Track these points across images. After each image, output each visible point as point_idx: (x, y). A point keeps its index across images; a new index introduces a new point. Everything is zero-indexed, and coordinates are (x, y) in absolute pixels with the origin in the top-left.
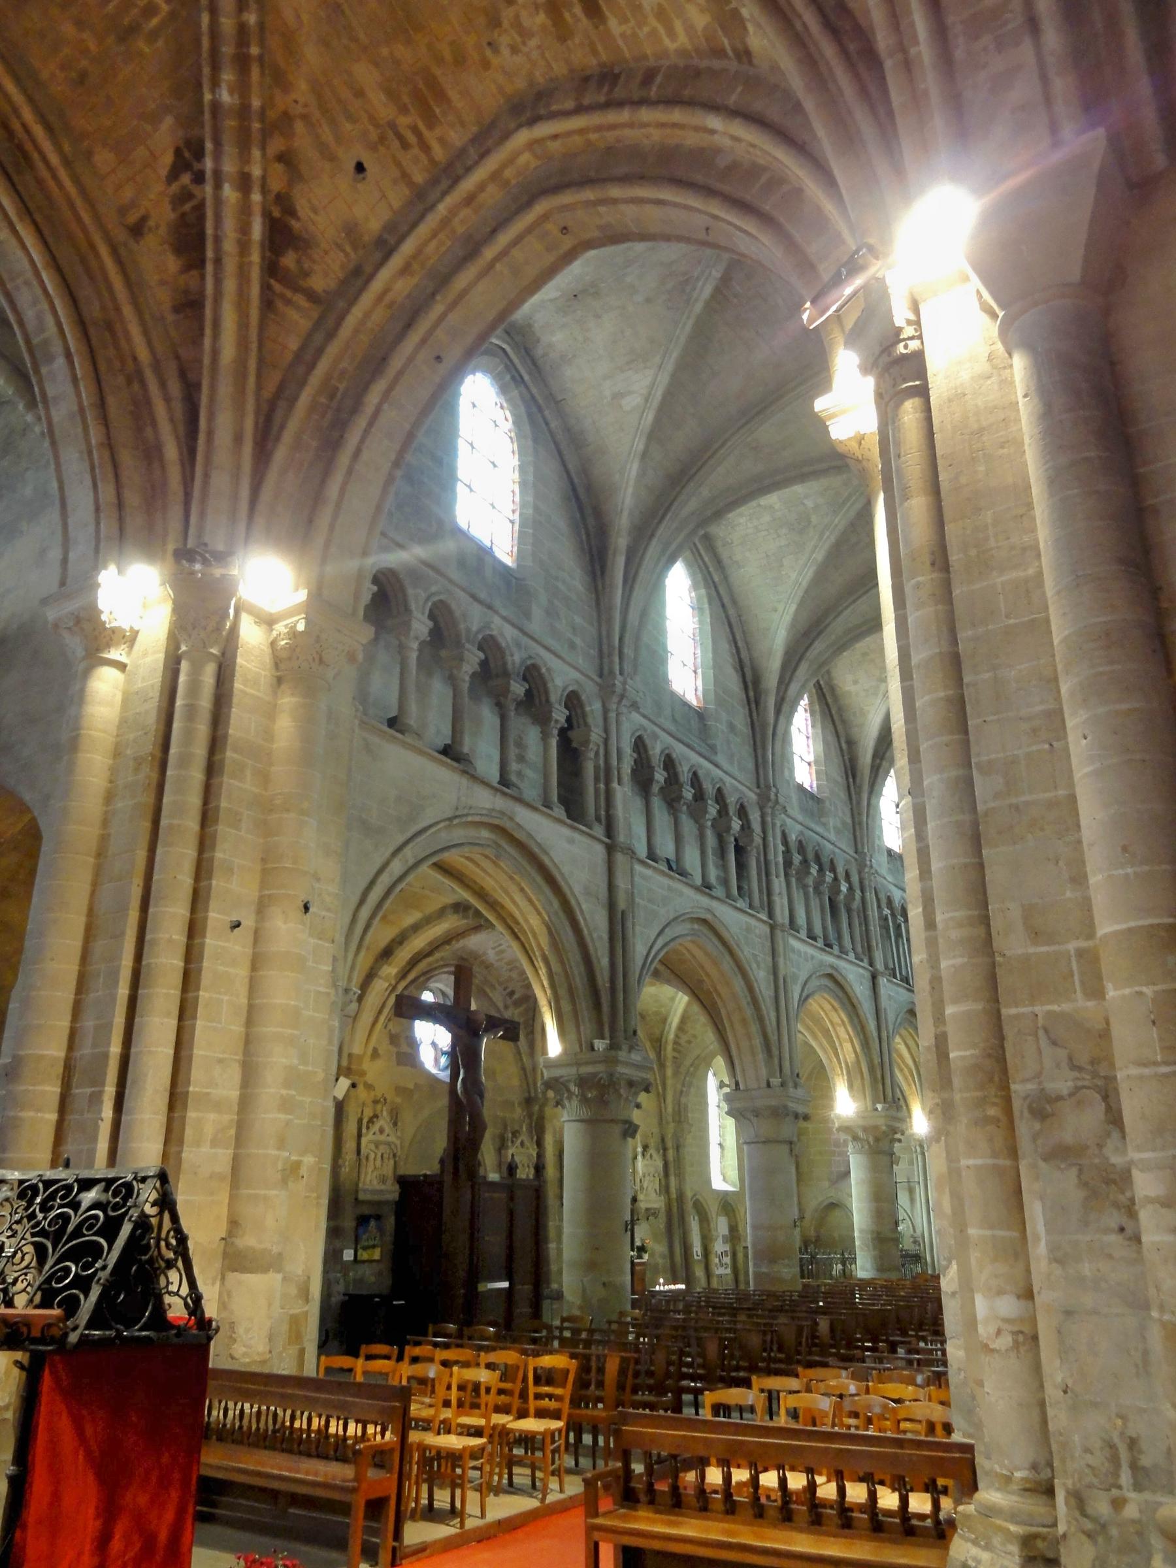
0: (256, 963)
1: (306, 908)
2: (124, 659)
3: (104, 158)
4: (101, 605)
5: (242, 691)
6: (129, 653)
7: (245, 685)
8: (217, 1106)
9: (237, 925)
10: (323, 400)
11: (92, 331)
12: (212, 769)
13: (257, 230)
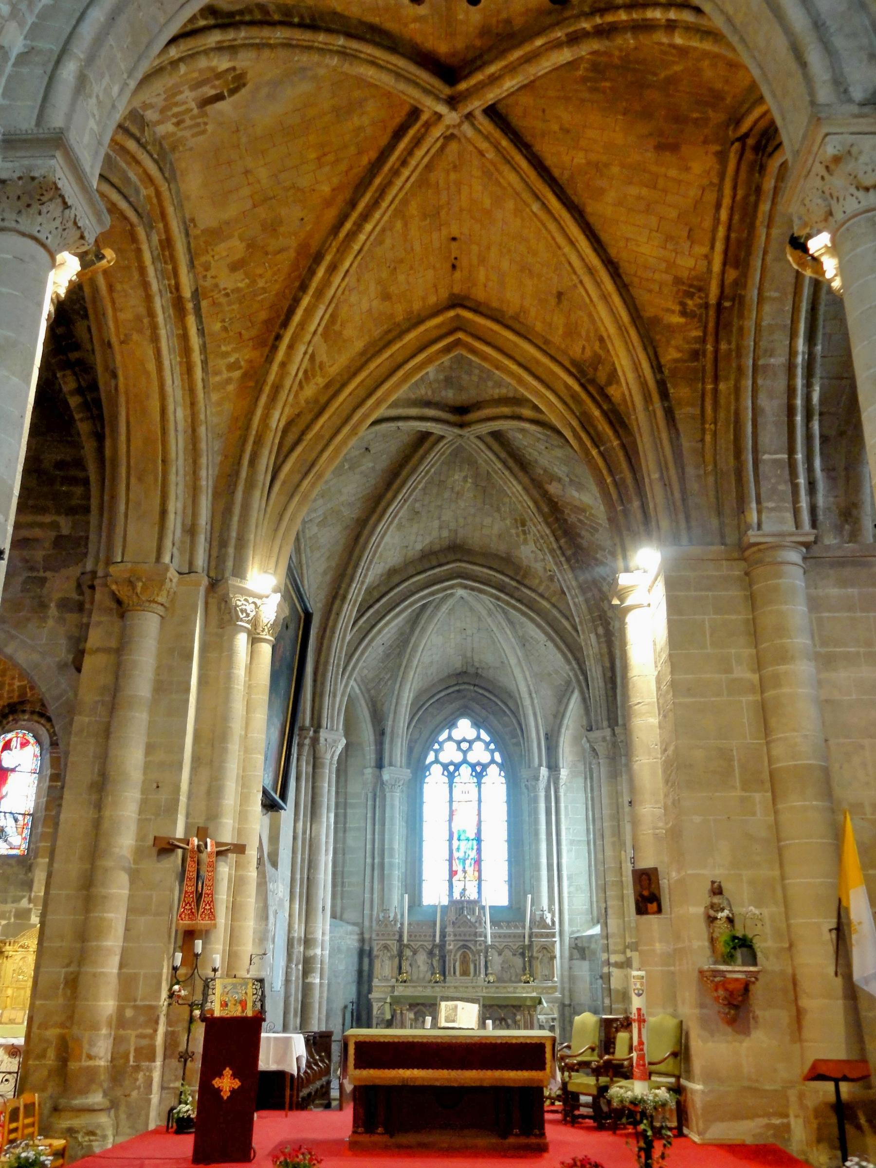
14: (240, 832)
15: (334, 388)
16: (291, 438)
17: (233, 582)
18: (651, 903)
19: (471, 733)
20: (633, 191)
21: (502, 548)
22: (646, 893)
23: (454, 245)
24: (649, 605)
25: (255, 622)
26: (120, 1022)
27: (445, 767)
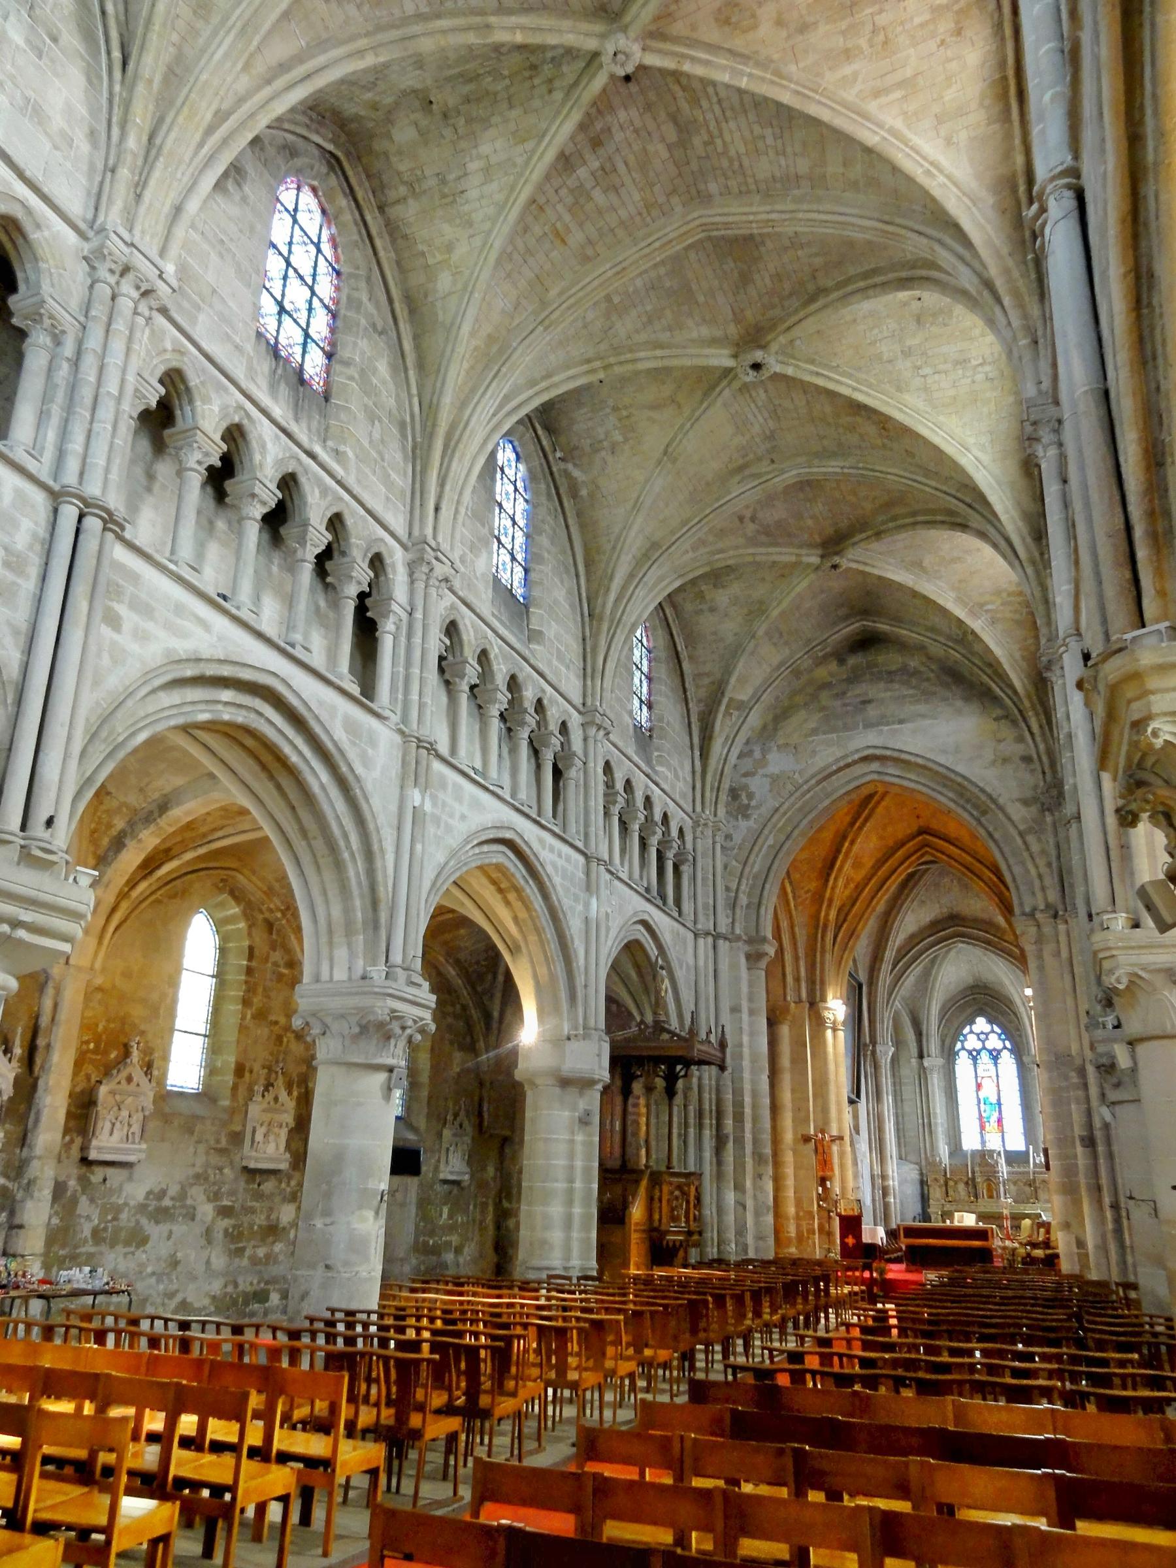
14: (840, 1129)
15: (859, 888)
16: (841, 918)
17: (822, 1005)
19: (987, 1028)
21: (985, 916)
25: (834, 1023)
26: (798, 1217)
27: (970, 1053)
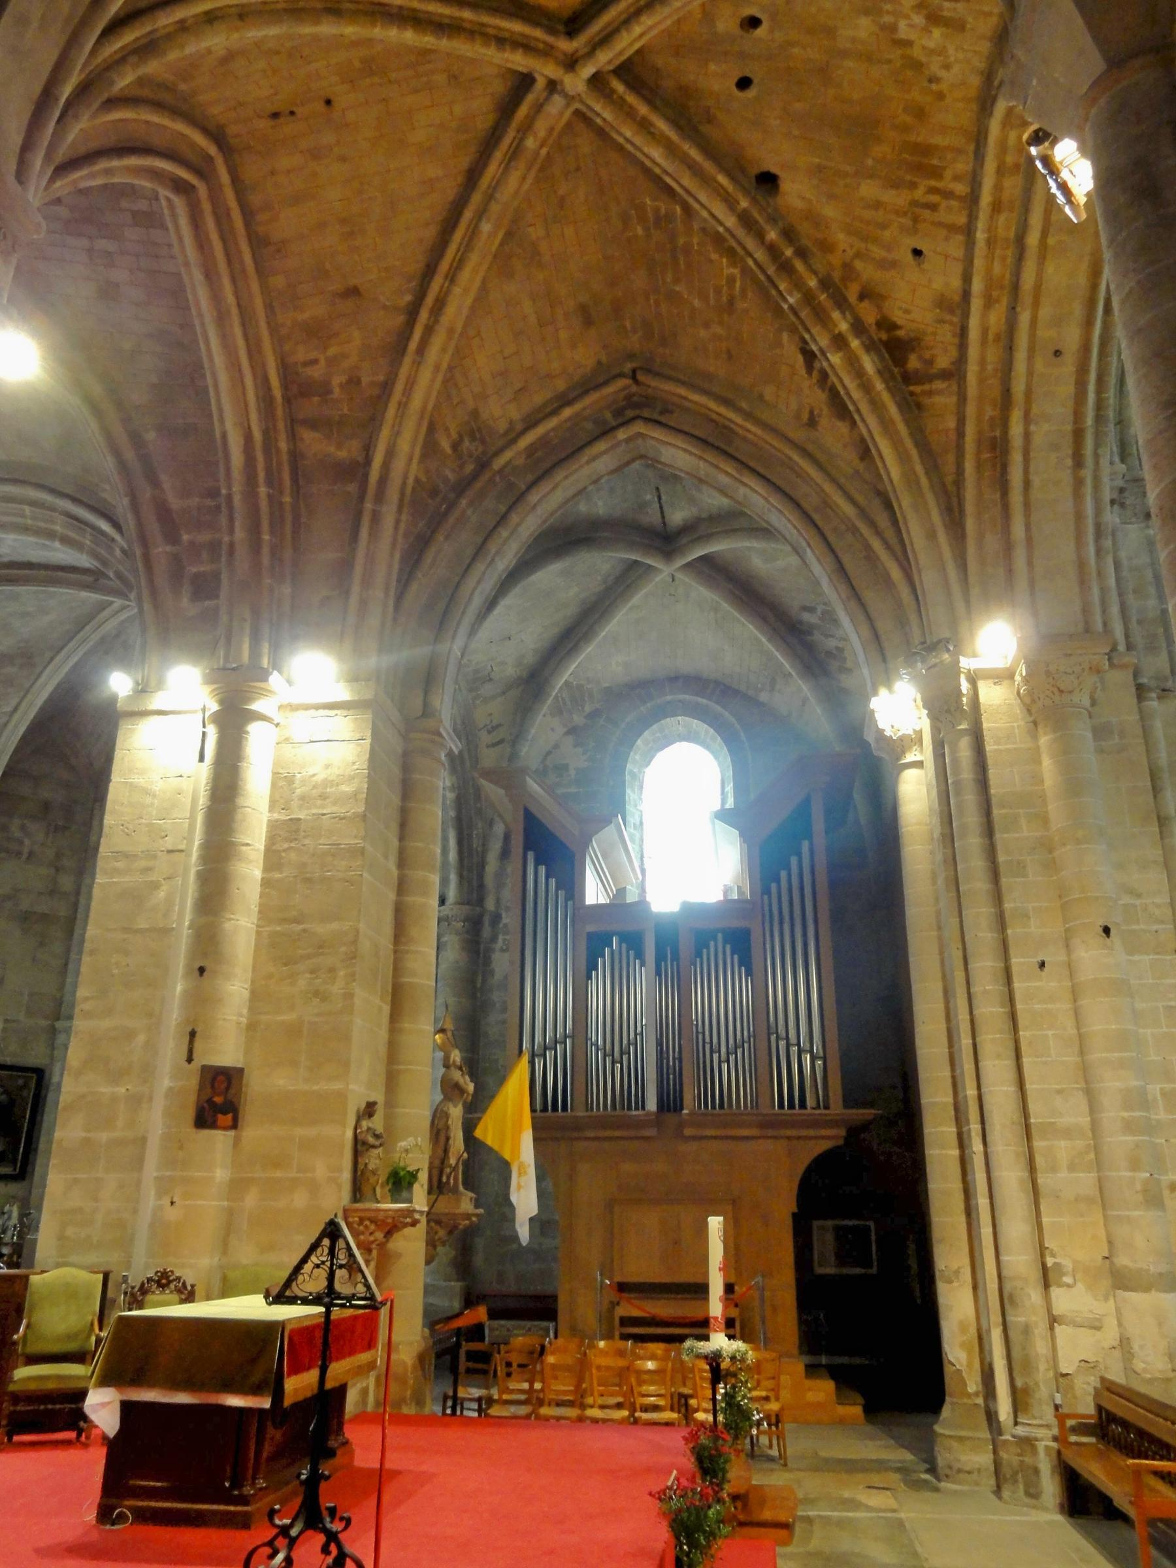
0: (1075, 993)
1: (1107, 931)
2: (919, 758)
3: (769, 392)
4: (881, 725)
5: (996, 750)
6: (921, 751)
7: (999, 744)
8: (1068, 1133)
9: (1042, 965)
10: (986, 456)
11: (816, 517)
12: (989, 830)
13: (869, 364)
18: (225, 1113)
20: (528, 307)
22: (218, 1100)
23: (320, 106)
24: (277, 725)
